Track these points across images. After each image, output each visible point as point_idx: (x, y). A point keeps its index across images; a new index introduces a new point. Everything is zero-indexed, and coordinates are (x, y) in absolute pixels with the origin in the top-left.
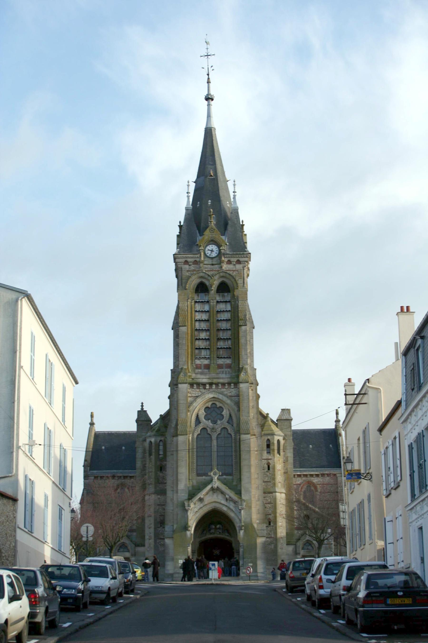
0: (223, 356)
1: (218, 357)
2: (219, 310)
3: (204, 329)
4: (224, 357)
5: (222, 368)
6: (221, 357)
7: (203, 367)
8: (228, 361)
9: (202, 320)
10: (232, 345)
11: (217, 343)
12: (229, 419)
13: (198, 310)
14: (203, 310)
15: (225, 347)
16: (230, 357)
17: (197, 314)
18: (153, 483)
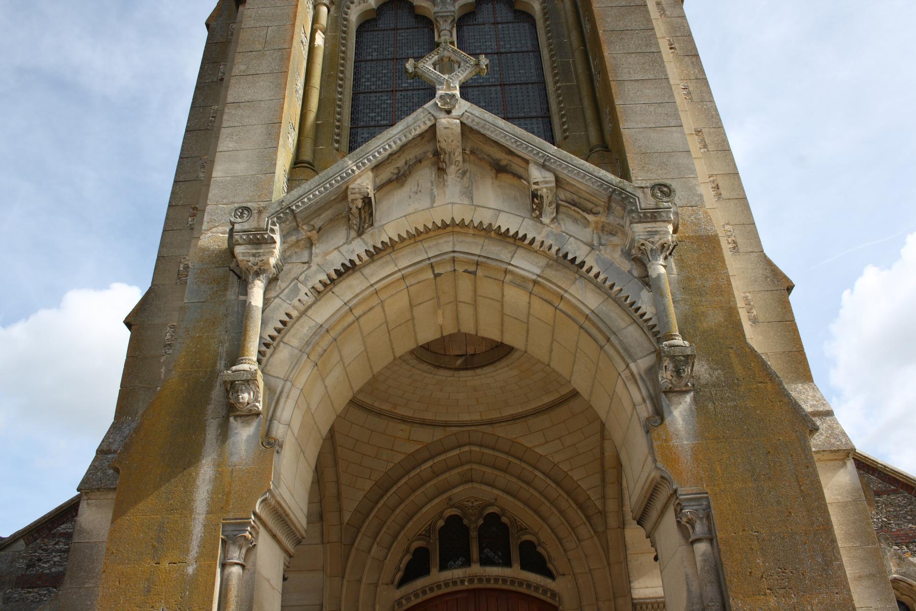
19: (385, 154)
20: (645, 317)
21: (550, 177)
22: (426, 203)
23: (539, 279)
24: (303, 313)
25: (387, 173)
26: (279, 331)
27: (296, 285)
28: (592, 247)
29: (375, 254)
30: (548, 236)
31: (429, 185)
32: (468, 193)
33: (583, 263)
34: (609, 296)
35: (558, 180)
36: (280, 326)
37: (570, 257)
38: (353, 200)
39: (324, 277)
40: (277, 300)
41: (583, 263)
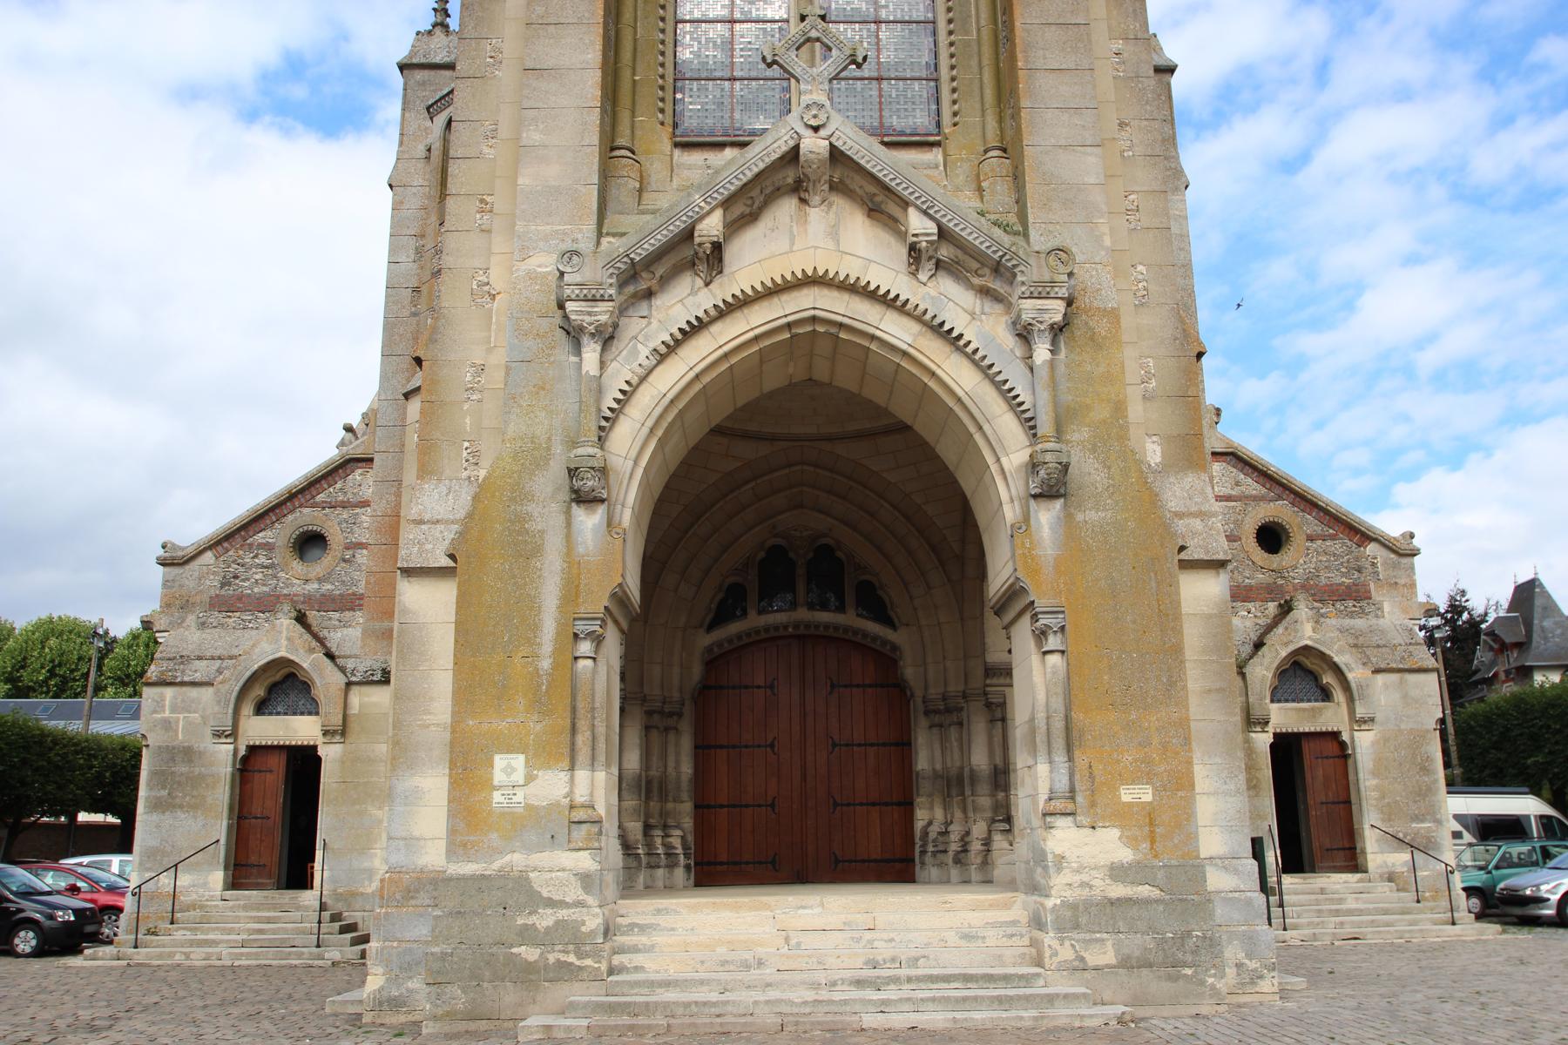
19: (738, 183)
20: (1023, 408)
21: (932, 228)
22: (784, 245)
23: (911, 351)
24: (643, 379)
25: (739, 209)
26: (618, 401)
27: (635, 347)
28: (972, 314)
29: (726, 311)
30: (923, 298)
31: (788, 219)
32: (834, 233)
33: (961, 336)
34: (987, 376)
35: (943, 233)
36: (621, 396)
37: (946, 328)
38: (700, 245)
39: (667, 338)
40: (614, 364)
41: (961, 336)
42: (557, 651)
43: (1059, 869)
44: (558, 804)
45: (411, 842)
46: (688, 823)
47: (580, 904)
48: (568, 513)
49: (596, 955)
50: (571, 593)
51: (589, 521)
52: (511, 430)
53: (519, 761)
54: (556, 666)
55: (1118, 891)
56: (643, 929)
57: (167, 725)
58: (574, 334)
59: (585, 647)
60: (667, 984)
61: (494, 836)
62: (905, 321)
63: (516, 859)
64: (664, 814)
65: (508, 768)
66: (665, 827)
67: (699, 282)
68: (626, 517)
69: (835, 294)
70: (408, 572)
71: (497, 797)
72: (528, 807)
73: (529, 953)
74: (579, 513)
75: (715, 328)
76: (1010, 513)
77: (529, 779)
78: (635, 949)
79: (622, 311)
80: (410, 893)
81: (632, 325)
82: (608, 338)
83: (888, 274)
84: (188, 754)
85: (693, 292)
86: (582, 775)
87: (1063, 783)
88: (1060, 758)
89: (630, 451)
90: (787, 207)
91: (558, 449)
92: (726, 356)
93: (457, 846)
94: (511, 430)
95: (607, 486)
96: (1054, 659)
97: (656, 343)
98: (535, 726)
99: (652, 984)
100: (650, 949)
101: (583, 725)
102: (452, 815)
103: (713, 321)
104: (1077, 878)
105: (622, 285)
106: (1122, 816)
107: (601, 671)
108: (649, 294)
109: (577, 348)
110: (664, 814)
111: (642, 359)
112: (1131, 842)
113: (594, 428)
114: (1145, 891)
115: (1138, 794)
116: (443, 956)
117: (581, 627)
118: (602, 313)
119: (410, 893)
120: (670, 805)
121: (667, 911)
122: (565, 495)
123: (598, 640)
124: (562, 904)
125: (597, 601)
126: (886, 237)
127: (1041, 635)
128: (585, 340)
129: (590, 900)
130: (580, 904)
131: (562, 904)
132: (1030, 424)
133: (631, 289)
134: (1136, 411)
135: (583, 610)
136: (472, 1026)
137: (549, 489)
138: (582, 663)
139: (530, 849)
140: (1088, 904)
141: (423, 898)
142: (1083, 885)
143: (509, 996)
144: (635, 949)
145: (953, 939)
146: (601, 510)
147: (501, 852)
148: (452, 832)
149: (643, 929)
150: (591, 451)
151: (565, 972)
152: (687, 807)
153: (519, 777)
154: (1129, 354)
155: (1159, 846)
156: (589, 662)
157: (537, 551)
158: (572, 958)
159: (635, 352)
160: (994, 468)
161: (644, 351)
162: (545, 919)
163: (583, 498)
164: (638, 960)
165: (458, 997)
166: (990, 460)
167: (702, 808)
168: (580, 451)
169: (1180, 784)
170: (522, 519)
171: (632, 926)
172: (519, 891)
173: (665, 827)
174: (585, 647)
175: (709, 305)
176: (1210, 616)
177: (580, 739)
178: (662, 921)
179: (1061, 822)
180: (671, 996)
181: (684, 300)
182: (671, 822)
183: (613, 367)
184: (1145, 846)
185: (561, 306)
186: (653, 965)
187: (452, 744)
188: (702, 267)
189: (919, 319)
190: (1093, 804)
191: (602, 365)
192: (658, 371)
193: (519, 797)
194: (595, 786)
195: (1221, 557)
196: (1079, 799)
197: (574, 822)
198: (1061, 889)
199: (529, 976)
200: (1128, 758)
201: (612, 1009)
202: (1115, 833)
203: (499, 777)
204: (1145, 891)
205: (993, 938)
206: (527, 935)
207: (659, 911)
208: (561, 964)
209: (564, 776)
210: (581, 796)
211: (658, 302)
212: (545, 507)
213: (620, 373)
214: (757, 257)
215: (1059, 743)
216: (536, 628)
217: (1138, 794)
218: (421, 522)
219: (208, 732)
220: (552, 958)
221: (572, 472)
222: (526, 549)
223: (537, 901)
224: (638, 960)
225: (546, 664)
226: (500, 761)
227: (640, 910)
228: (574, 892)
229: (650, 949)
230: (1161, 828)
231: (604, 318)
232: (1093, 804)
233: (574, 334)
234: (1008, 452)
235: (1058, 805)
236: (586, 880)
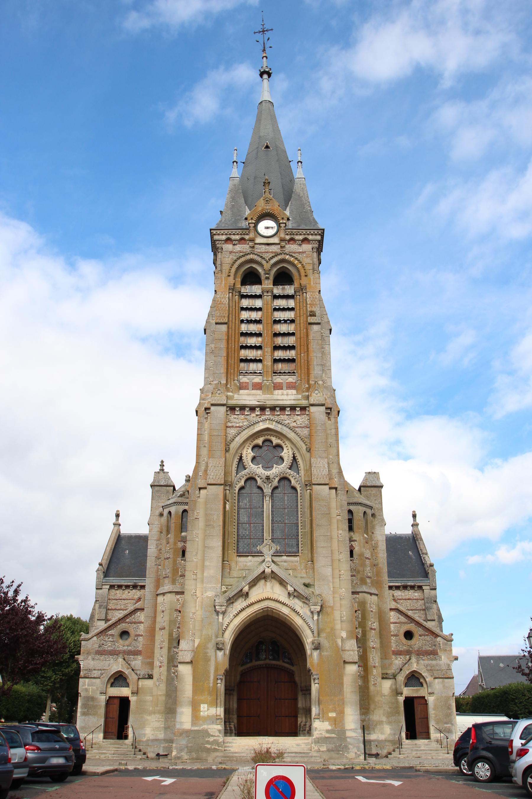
0: (282, 371)
1: (274, 373)
2: (277, 307)
3: (254, 332)
4: (285, 373)
5: (282, 389)
6: (280, 373)
7: (250, 387)
8: (291, 379)
9: (251, 320)
10: (296, 356)
11: (274, 352)
12: (292, 463)
13: (245, 307)
14: (253, 307)
15: (287, 358)
16: (294, 373)
17: (243, 313)
18: (170, 575)
42: (214, 682)
43: (316, 730)
44: (214, 715)
45: (181, 723)
46: (235, 721)
47: (218, 736)
48: (216, 652)
49: (222, 747)
50: (216, 670)
51: (220, 654)
52: (204, 633)
53: (206, 706)
54: (213, 685)
55: (328, 735)
56: (230, 743)
57: (87, 690)
58: (217, 613)
59: (219, 681)
60: (236, 753)
61: (201, 721)
62: (287, 608)
63: (205, 727)
64: (229, 718)
65: (204, 707)
66: (229, 722)
67: (243, 600)
68: (228, 652)
69: (272, 602)
70: (180, 663)
71: (202, 713)
72: (208, 715)
73: (208, 746)
74: (218, 652)
75: (246, 610)
76: (308, 652)
77: (208, 709)
78: (229, 747)
79: (227, 606)
80: (181, 734)
81: (229, 609)
82: (224, 613)
83: (283, 598)
84: (93, 699)
85: (242, 602)
86: (218, 709)
87: (318, 712)
88: (317, 707)
89: (228, 637)
90: (262, 582)
91: (214, 638)
92: (249, 616)
93: (193, 724)
94: (204, 633)
95: (224, 646)
96: (317, 685)
97: (234, 614)
98: (209, 698)
99: (233, 753)
100: (232, 747)
101: (219, 698)
102: (192, 717)
103: (246, 608)
104: (319, 732)
105: (227, 601)
106: (329, 719)
107: (221, 686)
108: (233, 603)
109: (218, 615)
110: (229, 718)
111: (231, 617)
112: (331, 725)
113: (221, 633)
114: (333, 735)
115: (332, 715)
116: (191, 746)
117: (218, 677)
118: (223, 608)
119: (181, 734)
120: (231, 716)
121: (235, 739)
122: (215, 648)
123: (221, 679)
124: (215, 736)
125: (222, 671)
126: (284, 589)
127: (314, 679)
128: (220, 614)
129: (220, 735)
130: (218, 736)
131: (215, 736)
132: (313, 632)
133: (229, 602)
134: (338, 626)
135: (219, 673)
136: (197, 761)
137: (212, 647)
138: (219, 685)
139: (208, 724)
140: (321, 738)
141: (184, 735)
142: (321, 734)
143: (204, 755)
144: (229, 747)
145: (295, 746)
146: (223, 651)
147: (202, 725)
148: (192, 720)
149: (230, 743)
150: (221, 639)
151: (215, 750)
152: (235, 716)
153: (206, 709)
154: (337, 615)
155: (336, 726)
156: (220, 685)
157: (209, 660)
158: (217, 747)
159: (230, 616)
160: (306, 642)
161: (232, 615)
162: (211, 739)
163: (220, 649)
164: (230, 749)
165: (194, 755)
166: (305, 640)
167: (239, 717)
168: (218, 639)
169: (341, 713)
170: (206, 653)
171: (228, 742)
172: (206, 733)
173: (229, 722)
174: (219, 681)
175: (245, 605)
176: (353, 675)
177: (218, 701)
178: (234, 741)
179: (317, 720)
180: (237, 755)
181: (240, 604)
182: (231, 721)
183: (225, 619)
184: (334, 726)
185: (215, 606)
186: (232, 750)
187: (192, 702)
188: (244, 597)
189: (290, 608)
190: (323, 717)
191: (223, 619)
192: (234, 620)
193: (206, 713)
194: (220, 711)
195: (356, 661)
196: (320, 716)
197: (214, 719)
198: (316, 734)
199: (208, 751)
200: (331, 707)
201: (225, 757)
202: (328, 723)
203: (202, 709)
204: (333, 735)
205: (303, 746)
206: (208, 742)
207: (233, 739)
208: (215, 749)
209: (215, 709)
210: (218, 714)
211: (234, 604)
212: (211, 651)
213: (227, 620)
214: (256, 593)
215: (317, 703)
216: (209, 677)
217: (332, 715)
218: (182, 651)
219: (99, 692)
220: (213, 747)
221: (217, 644)
222: (207, 660)
223: (210, 735)
224: (230, 749)
225: (211, 685)
226: (202, 706)
227: (230, 739)
228: (217, 734)
229: (232, 747)
230: (338, 723)
231: (224, 610)
232: (323, 717)
233: (217, 613)
234: (308, 639)
235: (316, 717)
236: (220, 731)
